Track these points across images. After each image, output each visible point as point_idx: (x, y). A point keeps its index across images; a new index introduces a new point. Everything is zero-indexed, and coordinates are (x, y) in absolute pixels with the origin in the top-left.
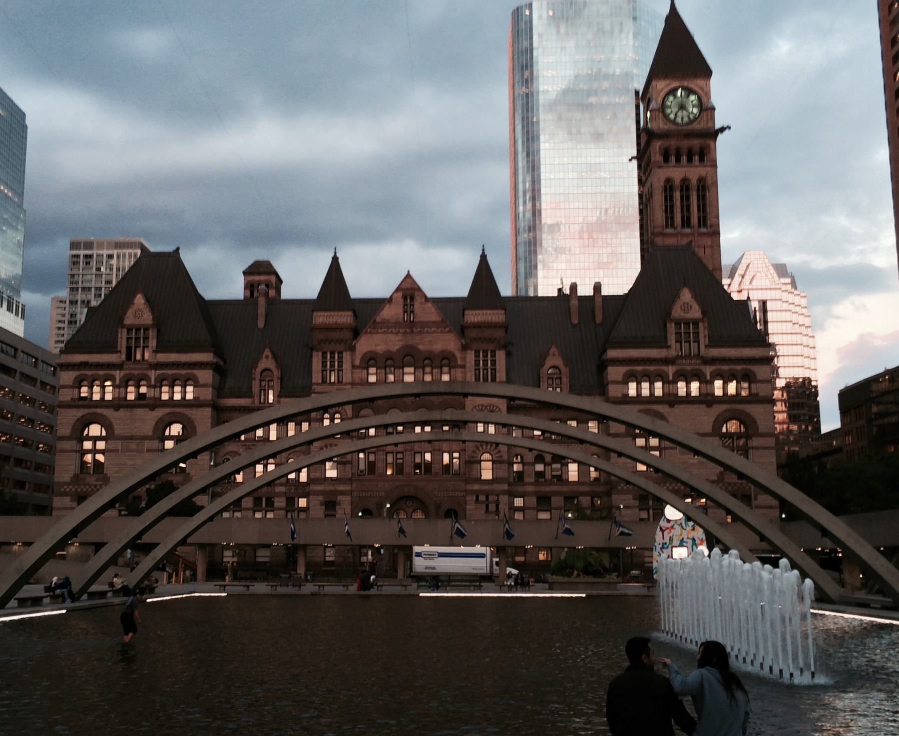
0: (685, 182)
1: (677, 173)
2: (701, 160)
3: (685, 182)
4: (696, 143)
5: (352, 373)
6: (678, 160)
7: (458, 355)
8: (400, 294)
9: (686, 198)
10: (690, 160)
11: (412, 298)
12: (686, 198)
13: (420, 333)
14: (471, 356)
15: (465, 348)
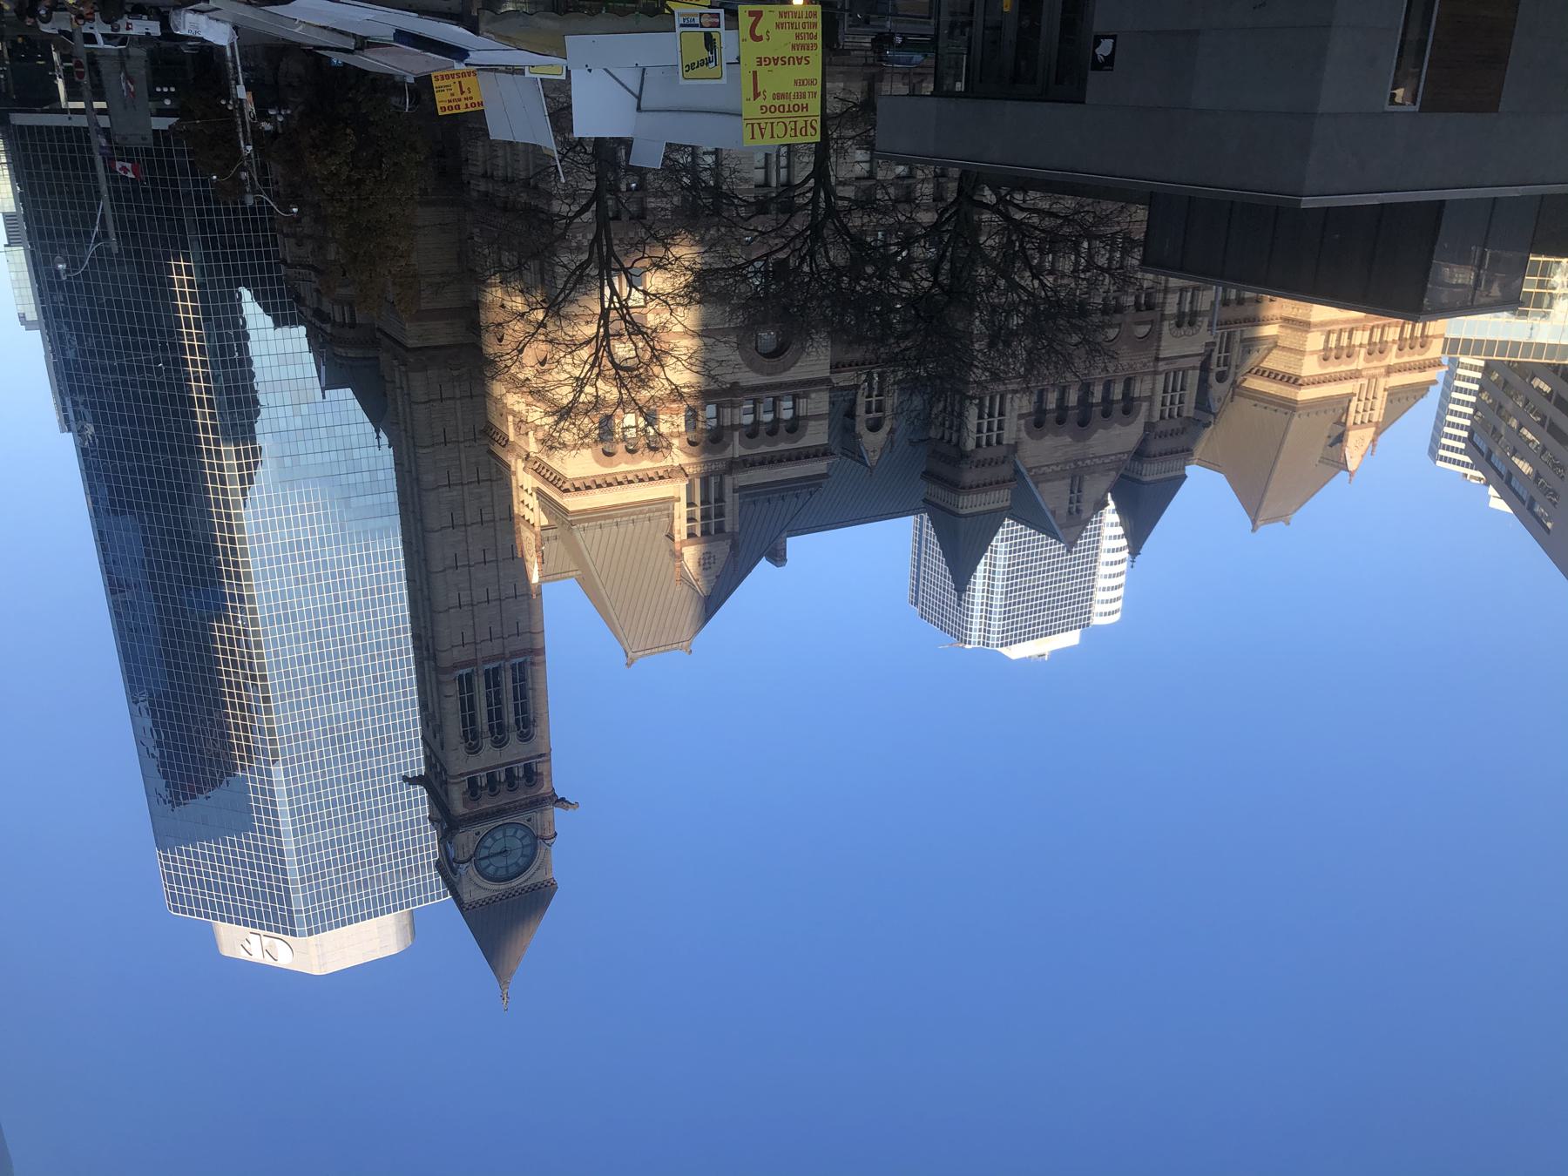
0: (499, 743)
1: (515, 750)
2: (472, 782)
3: (499, 743)
4: (487, 803)
5: (1153, 389)
6: (509, 772)
7: (1023, 435)
8: (1084, 516)
9: (496, 714)
10: (491, 778)
11: (1070, 512)
12: (496, 714)
13: (1066, 462)
14: (1008, 437)
15: (1014, 448)
